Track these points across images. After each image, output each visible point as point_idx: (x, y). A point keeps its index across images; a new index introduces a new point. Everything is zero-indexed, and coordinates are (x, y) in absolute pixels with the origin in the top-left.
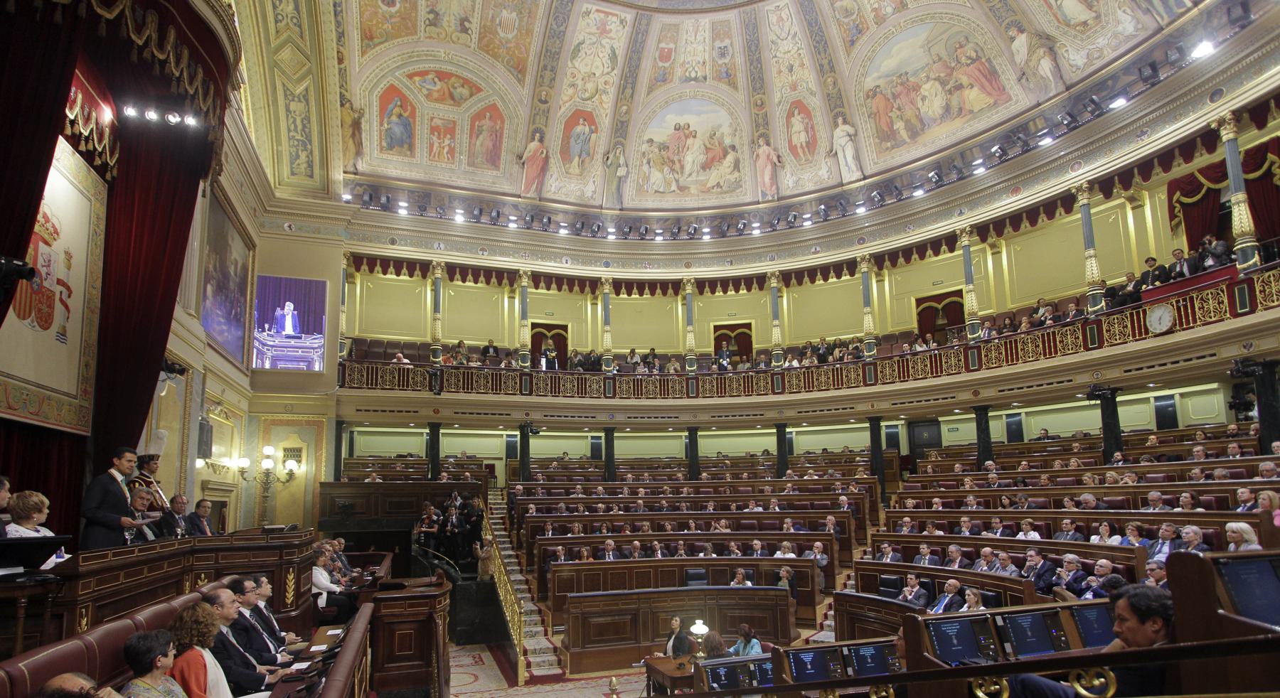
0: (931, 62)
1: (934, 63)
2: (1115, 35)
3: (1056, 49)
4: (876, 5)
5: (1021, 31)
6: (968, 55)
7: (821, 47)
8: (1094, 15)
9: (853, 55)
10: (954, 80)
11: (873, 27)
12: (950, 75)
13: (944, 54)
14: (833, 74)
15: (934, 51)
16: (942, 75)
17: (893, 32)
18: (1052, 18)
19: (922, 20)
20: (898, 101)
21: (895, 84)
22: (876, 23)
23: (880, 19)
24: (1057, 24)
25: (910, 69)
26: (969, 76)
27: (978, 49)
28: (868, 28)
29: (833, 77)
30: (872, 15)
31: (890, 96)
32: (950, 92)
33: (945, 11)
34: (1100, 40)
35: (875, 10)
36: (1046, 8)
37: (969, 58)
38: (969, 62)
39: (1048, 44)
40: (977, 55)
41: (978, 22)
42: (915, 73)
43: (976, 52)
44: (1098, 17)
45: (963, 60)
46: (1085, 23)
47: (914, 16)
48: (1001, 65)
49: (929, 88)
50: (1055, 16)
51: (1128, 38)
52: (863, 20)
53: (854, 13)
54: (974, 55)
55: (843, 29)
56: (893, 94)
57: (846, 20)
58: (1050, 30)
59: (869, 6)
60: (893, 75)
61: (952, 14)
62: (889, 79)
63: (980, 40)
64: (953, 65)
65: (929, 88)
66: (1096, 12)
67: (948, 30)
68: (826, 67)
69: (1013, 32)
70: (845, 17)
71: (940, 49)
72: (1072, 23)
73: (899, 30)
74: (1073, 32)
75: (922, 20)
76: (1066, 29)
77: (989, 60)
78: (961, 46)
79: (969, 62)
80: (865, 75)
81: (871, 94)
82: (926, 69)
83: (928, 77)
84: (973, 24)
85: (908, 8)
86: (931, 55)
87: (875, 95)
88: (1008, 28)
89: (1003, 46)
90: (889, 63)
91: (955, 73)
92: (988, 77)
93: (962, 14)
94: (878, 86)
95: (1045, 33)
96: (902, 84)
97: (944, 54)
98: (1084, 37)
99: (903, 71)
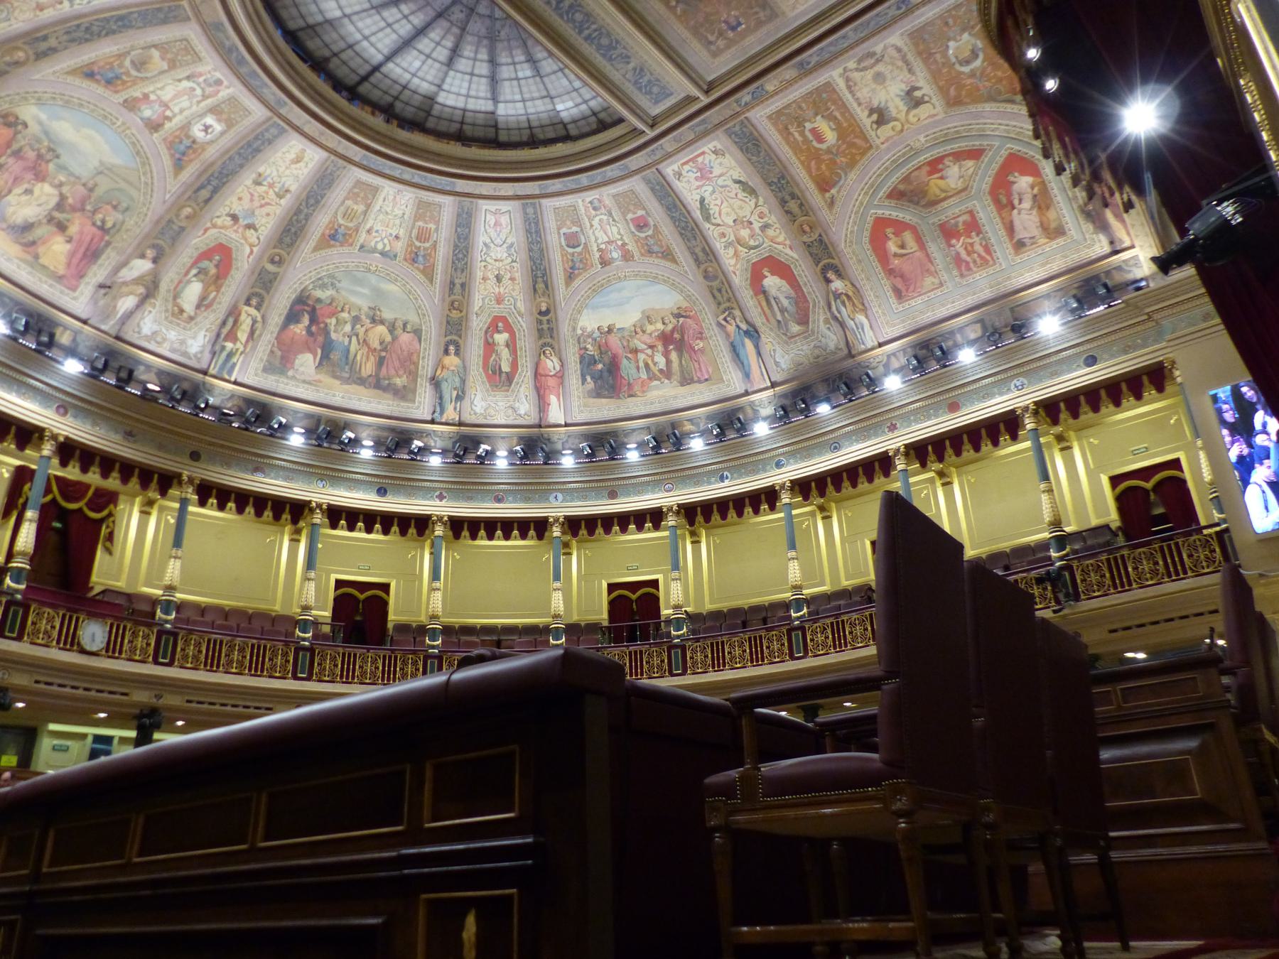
0: (83, 181)
1: (84, 185)
2: (183, 342)
3: (148, 301)
4: (153, 97)
5: (155, 261)
6: (107, 218)
7: (81, 34)
8: (192, 314)
9: (70, 79)
10: (69, 216)
11: (120, 98)
12: (74, 209)
13: (99, 191)
14: (32, 57)
15: (99, 179)
16: (70, 201)
17: (115, 124)
18: (176, 282)
19: (138, 153)
20: (11, 161)
21: (37, 146)
22: (125, 101)
23: (131, 105)
24: (172, 288)
25: (65, 159)
26: (81, 233)
27: (117, 227)
28: (117, 92)
29: (28, 59)
30: (138, 94)
31: (15, 146)
32: (50, 220)
33: (155, 174)
34: (173, 333)
35: (146, 96)
36: (183, 271)
37: (103, 222)
38: (99, 223)
39: (150, 288)
40: (110, 229)
41: (150, 214)
42: (62, 168)
43: (114, 225)
44: (191, 318)
45: (99, 216)
46: (182, 311)
47: (143, 143)
48: (108, 260)
49: (46, 193)
50: (180, 282)
51: (185, 354)
52: (129, 84)
53: (138, 71)
54: (109, 225)
55: (112, 60)
56: (20, 150)
57: (127, 63)
58: (164, 286)
59: (151, 89)
60: (50, 140)
61: (152, 183)
62: (43, 137)
63: (130, 222)
64: (88, 208)
65: (46, 193)
66: (196, 314)
67: (131, 184)
68: (43, 46)
69: (150, 253)
70: (133, 62)
71: (104, 185)
72: (179, 301)
73: (120, 130)
74: (170, 307)
75: (138, 153)
76: (171, 299)
77: (108, 244)
78: (115, 207)
79: (99, 223)
80: (40, 102)
81: (11, 119)
82: (72, 179)
83: (61, 185)
84: (145, 209)
85: (151, 133)
86: (93, 178)
87: (9, 125)
88: (154, 246)
89: (129, 250)
90: (66, 129)
91: (78, 214)
92: (89, 253)
93: (155, 195)
94: (26, 125)
95: (159, 282)
96: (40, 156)
97: (99, 191)
98: (170, 318)
99: (60, 151)
